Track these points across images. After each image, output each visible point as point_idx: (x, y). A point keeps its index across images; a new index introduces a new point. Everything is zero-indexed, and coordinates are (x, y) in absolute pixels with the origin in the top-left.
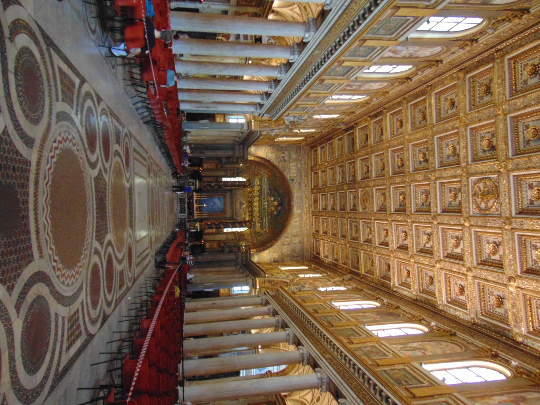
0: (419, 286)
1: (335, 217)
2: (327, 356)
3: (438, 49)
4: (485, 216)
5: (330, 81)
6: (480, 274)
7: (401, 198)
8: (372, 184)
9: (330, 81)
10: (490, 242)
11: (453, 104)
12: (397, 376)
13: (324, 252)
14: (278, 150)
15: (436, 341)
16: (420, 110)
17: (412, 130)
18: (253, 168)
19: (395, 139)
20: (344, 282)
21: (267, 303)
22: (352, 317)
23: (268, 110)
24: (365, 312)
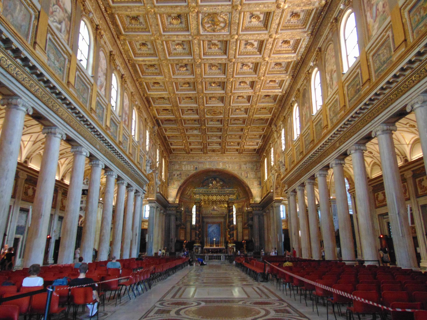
0: (283, 73)
1: (226, 136)
2: (338, 145)
3: (102, 54)
4: (230, 24)
5: (121, 136)
6: (274, 28)
7: (213, 85)
8: (202, 107)
9: (121, 136)
10: (250, 20)
11: (144, 44)
12: (353, 92)
13: (254, 145)
14: (172, 179)
15: (325, 62)
16: (147, 69)
17: (162, 75)
18: (185, 199)
19: (168, 88)
20: (278, 130)
21: (294, 191)
22: (306, 125)
23: (140, 187)
24: (302, 115)
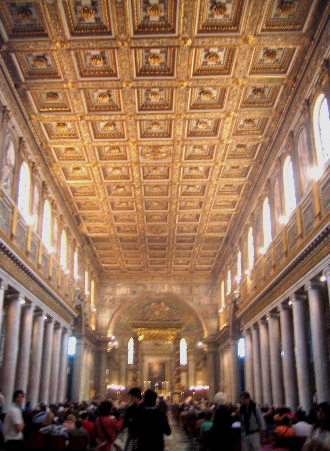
11: (78, 168)
17: (95, 195)
